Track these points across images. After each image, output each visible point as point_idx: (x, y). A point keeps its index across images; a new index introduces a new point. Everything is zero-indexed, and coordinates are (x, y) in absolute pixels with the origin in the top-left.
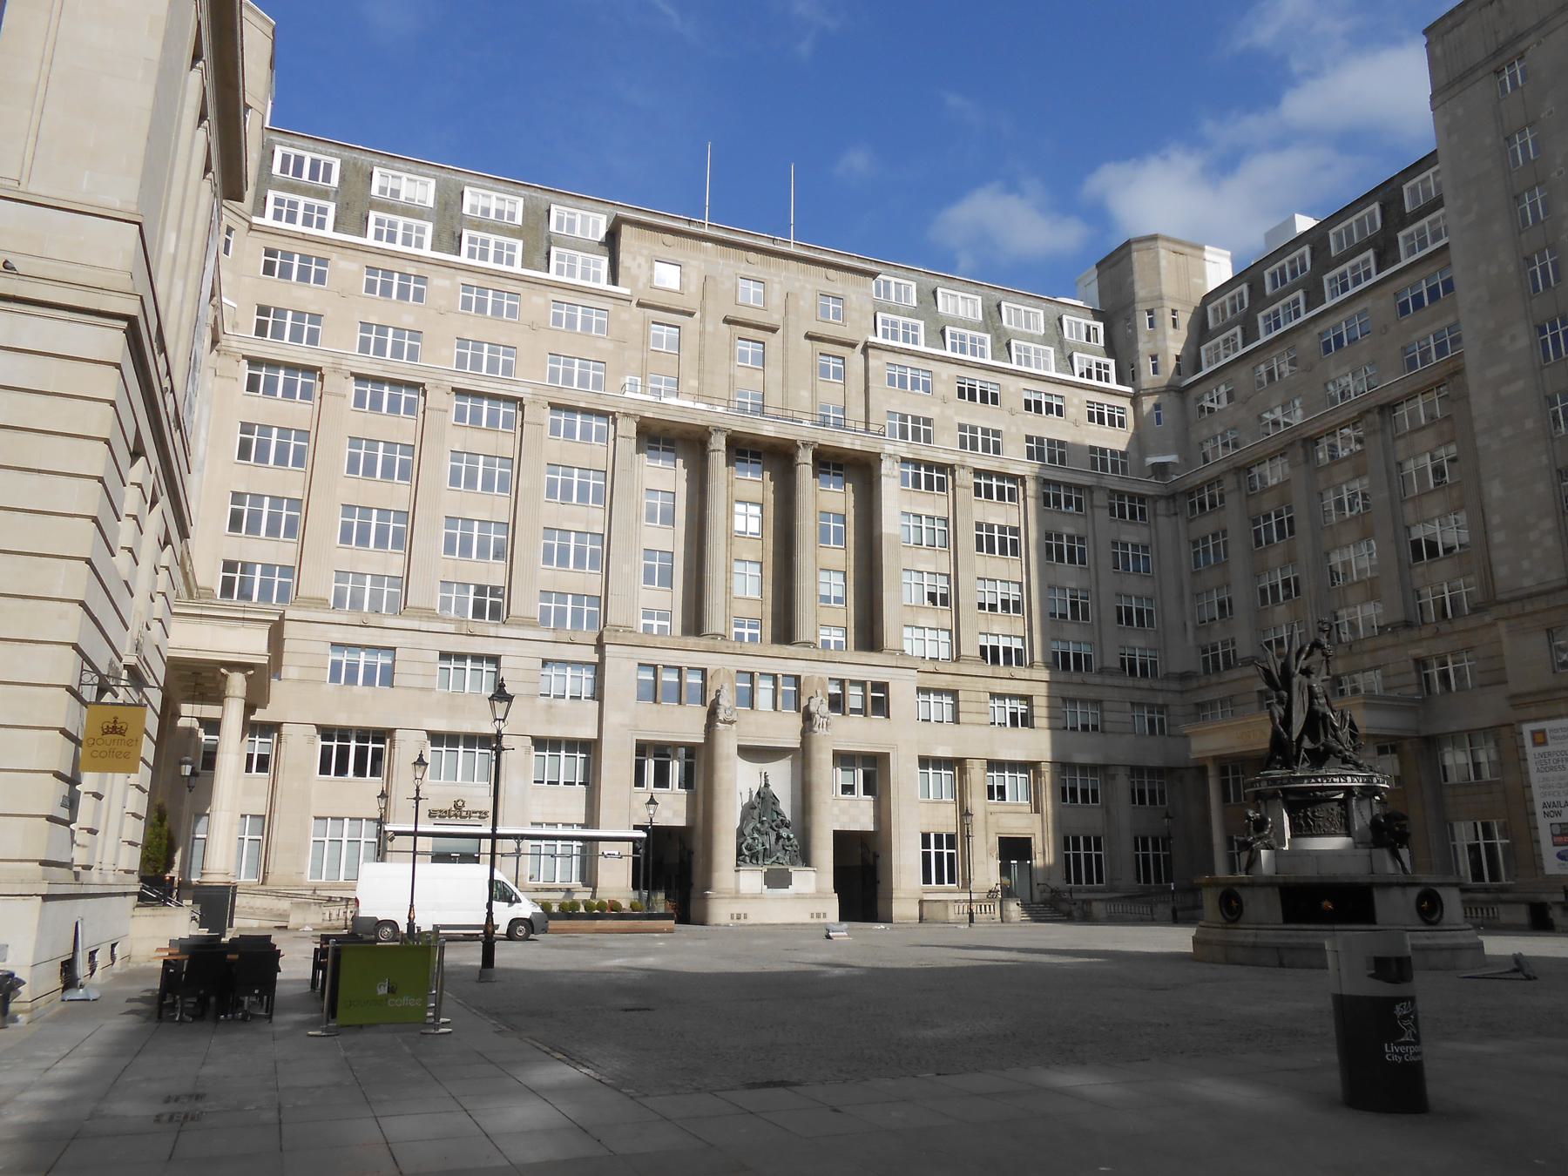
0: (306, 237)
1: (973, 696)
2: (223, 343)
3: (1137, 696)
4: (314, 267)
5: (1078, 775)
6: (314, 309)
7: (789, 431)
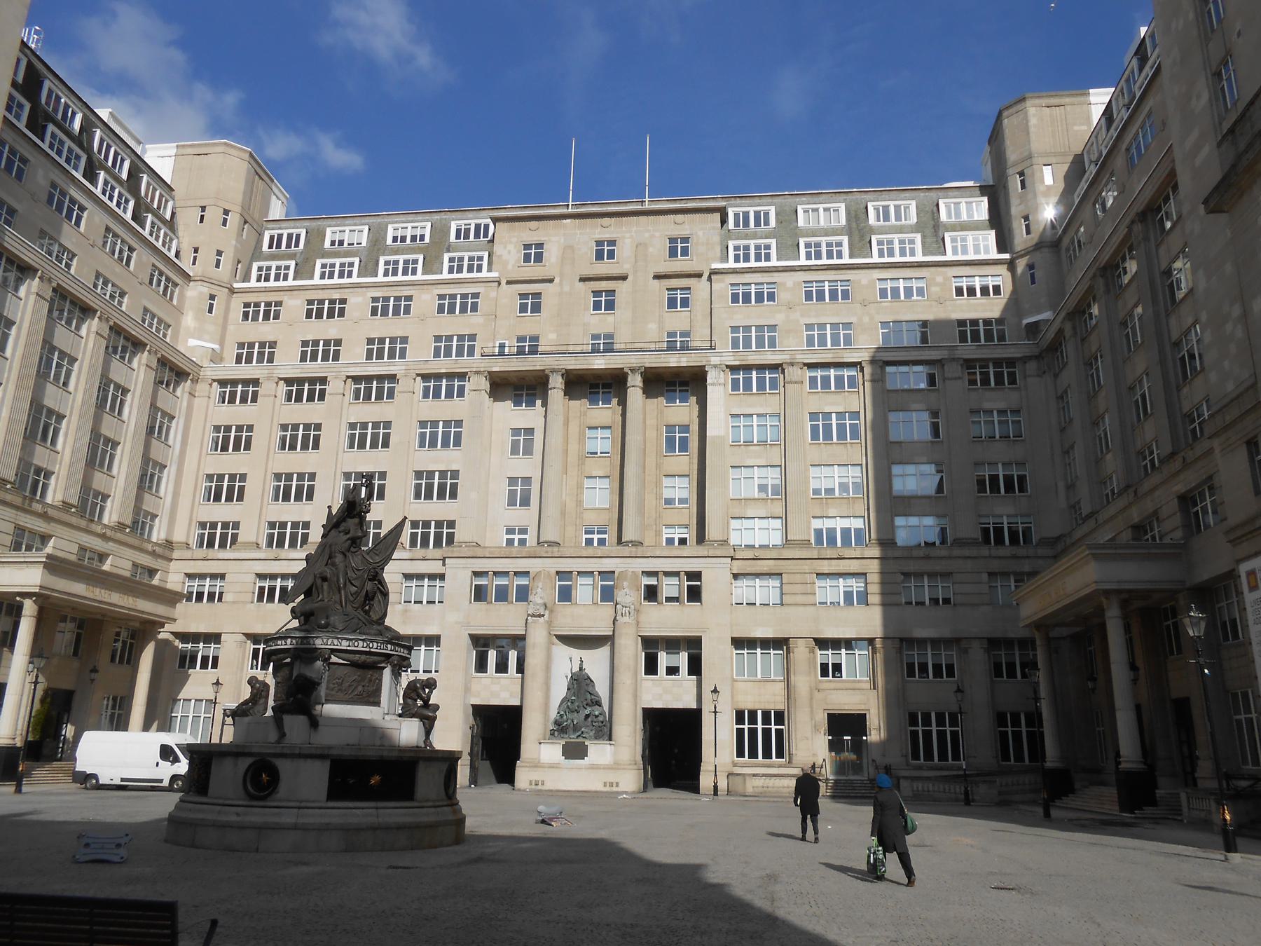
0: (267, 289)
1: (798, 578)
3: (996, 566)
4: (470, 301)
5: (929, 649)
7: (618, 361)
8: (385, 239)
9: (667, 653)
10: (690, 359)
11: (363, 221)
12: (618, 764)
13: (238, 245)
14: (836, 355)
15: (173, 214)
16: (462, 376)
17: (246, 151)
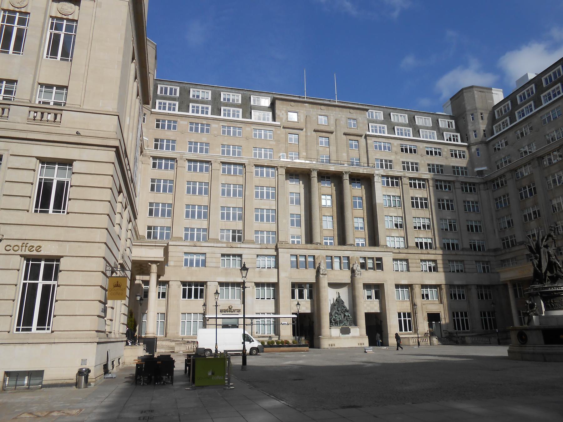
0: (169, 114)
1: (414, 261)
2: (144, 152)
6: (173, 138)
7: (340, 168)
9: (367, 290)
10: (368, 171)
11: (206, 88)
14: (419, 175)
17: (155, 44)
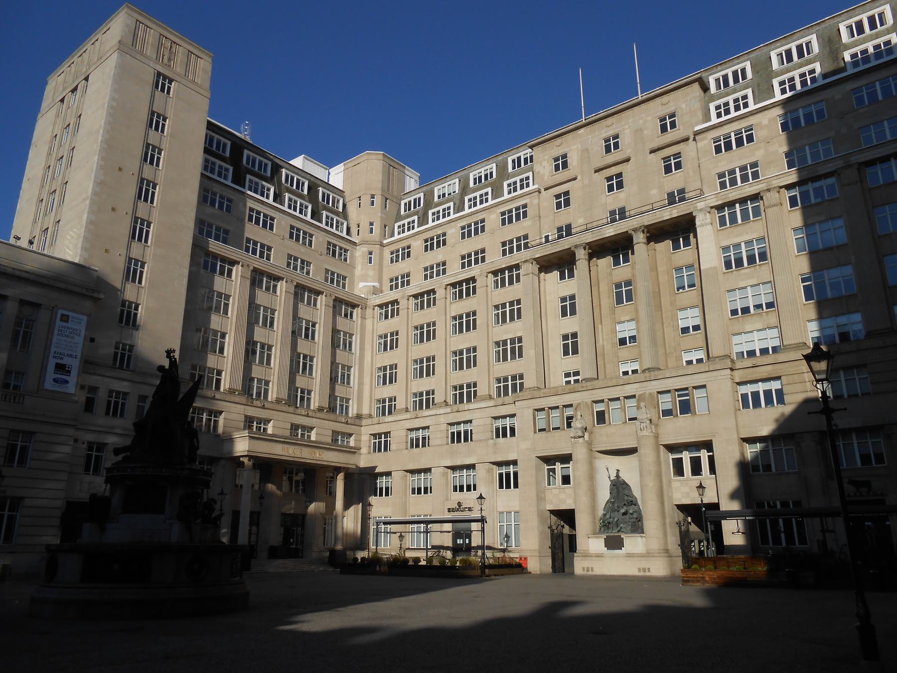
6: (406, 271)
8: (469, 184)
12: (649, 553)
13: (383, 215)
15: (344, 206)
16: (517, 267)
17: (381, 154)
